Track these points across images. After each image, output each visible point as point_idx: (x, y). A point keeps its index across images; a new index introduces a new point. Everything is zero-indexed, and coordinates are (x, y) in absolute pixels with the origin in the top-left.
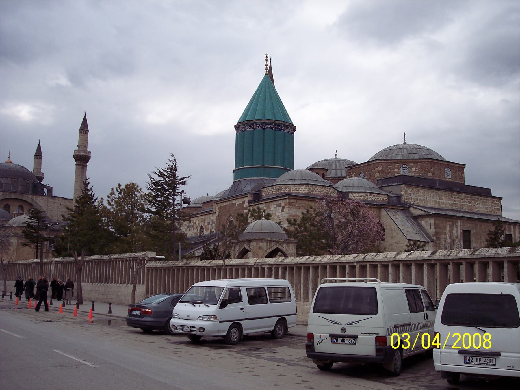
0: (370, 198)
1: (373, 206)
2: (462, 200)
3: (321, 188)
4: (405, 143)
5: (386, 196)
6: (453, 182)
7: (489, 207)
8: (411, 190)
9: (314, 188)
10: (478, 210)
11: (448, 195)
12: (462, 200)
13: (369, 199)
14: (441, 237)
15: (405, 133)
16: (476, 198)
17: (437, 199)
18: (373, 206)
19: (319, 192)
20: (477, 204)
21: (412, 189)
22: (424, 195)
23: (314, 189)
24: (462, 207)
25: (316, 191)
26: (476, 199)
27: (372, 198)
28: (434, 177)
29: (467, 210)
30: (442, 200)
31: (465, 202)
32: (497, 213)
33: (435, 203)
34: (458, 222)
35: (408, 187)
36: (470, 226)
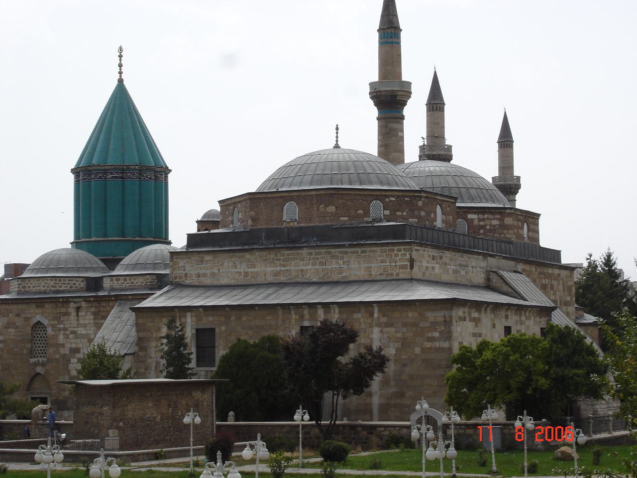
0: (118, 284)
1: (110, 299)
2: (301, 262)
3: (37, 281)
4: (337, 146)
5: (148, 276)
6: (301, 227)
7: (377, 265)
8: (187, 260)
9: (27, 282)
10: (343, 275)
11: (268, 258)
12: (303, 260)
13: (116, 286)
14: (149, 345)
15: (337, 125)
16: (339, 252)
17: (243, 268)
18: (110, 299)
19: (34, 287)
20: (344, 264)
21: (190, 258)
22: (214, 265)
23: (27, 284)
24: (302, 275)
25: (29, 287)
26: (340, 255)
27: (121, 283)
28: (255, 226)
29: (315, 280)
30: (254, 268)
31: (309, 265)
32: (398, 274)
33: (237, 276)
34: (185, 316)
35: (179, 256)
36: (214, 320)
